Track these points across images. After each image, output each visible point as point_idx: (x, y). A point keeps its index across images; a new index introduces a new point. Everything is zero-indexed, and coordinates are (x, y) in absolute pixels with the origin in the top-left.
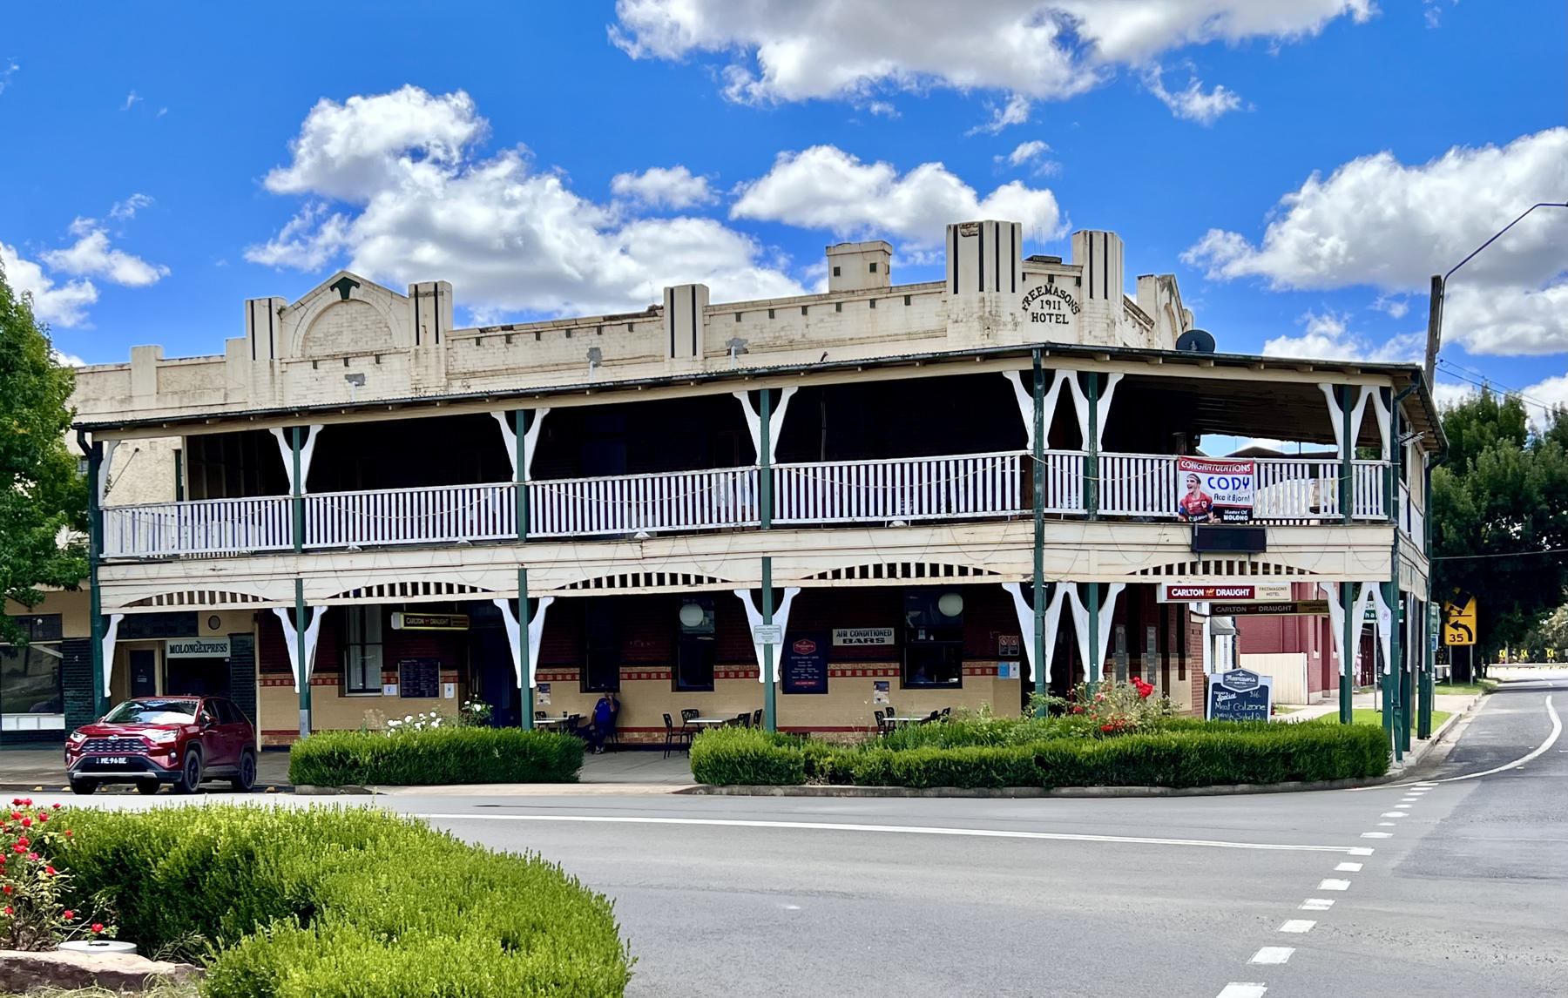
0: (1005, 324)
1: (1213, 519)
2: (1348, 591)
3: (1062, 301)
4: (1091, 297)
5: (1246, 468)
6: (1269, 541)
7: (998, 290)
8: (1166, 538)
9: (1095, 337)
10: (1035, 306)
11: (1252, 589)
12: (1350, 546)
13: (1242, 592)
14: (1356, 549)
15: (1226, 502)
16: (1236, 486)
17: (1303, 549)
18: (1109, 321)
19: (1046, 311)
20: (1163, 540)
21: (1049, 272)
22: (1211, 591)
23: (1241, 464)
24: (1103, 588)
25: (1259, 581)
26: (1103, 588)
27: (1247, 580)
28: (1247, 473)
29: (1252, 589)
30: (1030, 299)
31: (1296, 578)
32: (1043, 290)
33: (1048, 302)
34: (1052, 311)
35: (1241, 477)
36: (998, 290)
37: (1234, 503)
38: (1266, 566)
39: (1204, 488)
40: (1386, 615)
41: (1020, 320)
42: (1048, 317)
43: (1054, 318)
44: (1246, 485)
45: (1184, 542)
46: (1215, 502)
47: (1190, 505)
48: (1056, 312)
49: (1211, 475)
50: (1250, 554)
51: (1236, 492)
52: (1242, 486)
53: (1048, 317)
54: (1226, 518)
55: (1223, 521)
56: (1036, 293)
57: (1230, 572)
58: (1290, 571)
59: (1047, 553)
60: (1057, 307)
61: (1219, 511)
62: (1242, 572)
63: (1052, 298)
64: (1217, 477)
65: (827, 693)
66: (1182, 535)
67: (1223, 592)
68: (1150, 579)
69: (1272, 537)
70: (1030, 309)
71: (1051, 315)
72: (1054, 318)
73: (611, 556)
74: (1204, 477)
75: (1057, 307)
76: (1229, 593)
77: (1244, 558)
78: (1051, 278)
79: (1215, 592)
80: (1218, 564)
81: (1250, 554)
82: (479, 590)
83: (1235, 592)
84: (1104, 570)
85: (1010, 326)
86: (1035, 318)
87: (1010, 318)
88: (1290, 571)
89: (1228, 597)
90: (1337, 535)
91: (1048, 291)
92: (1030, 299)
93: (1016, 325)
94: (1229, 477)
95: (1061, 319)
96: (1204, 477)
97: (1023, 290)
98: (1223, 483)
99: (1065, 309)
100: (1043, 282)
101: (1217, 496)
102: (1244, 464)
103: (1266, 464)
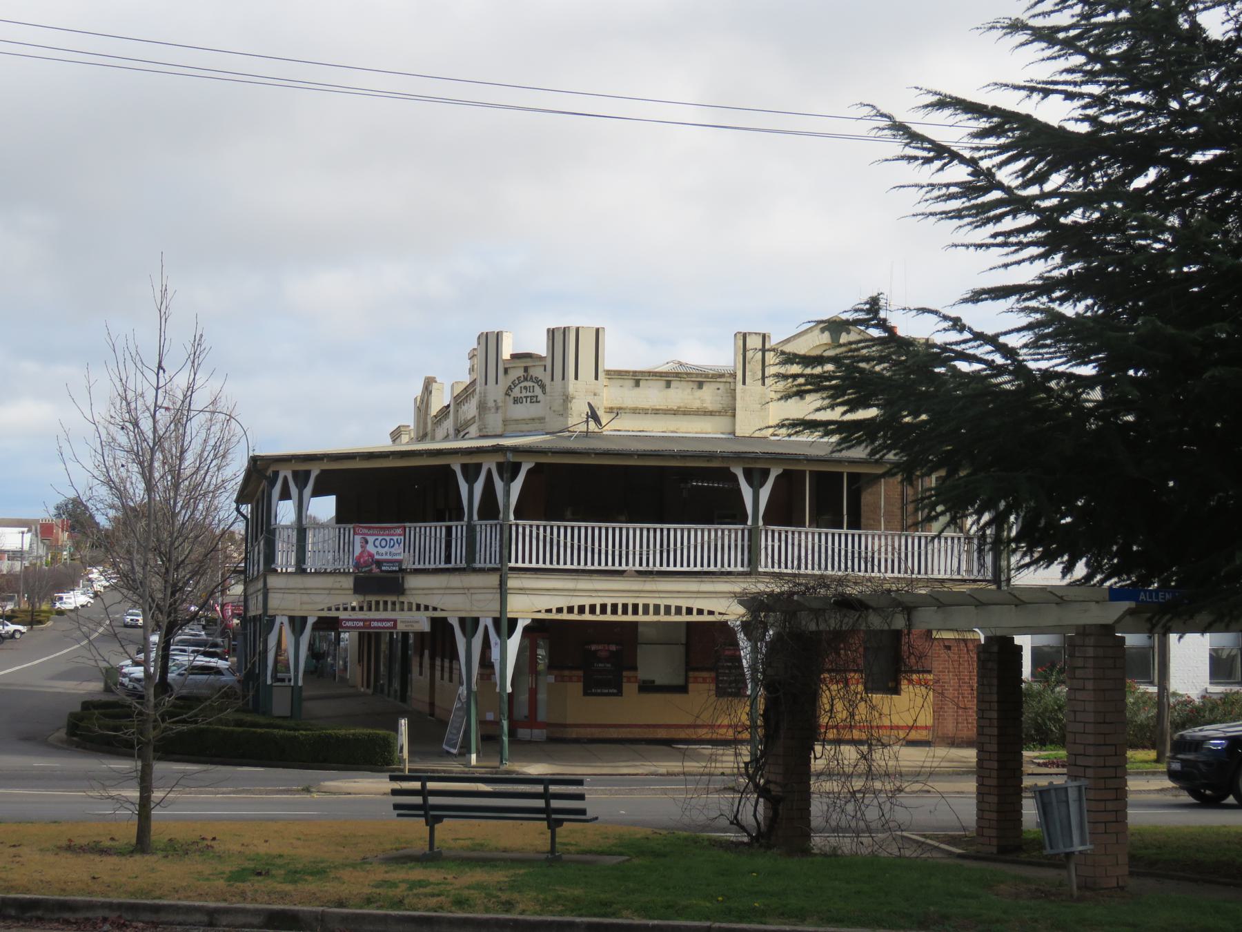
0: (490, 409)
2: (469, 625)
3: (536, 385)
4: (552, 379)
5: (399, 531)
6: (406, 586)
7: (486, 384)
9: (554, 411)
10: (516, 392)
11: (395, 621)
12: (468, 589)
13: (388, 624)
14: (472, 591)
15: (384, 557)
16: (392, 544)
17: (435, 592)
19: (524, 394)
20: (337, 585)
21: (525, 365)
22: (368, 623)
23: (392, 528)
24: (304, 619)
25: (406, 615)
26: (304, 619)
28: (400, 535)
29: (395, 621)
30: (513, 387)
31: (431, 614)
32: (522, 379)
33: (525, 388)
35: (395, 538)
36: (486, 384)
37: (390, 558)
38: (410, 604)
40: (496, 644)
41: (500, 404)
42: (524, 400)
43: (529, 399)
46: (377, 557)
47: (362, 560)
51: (393, 550)
52: (397, 545)
53: (524, 400)
54: (383, 568)
55: (382, 571)
56: (517, 382)
57: (385, 609)
58: (427, 608)
59: (271, 595)
61: (379, 563)
62: (377, 609)
63: (531, 384)
64: (380, 538)
65: (622, 696)
66: (348, 582)
67: (375, 624)
68: (333, 614)
69: (412, 582)
70: (513, 395)
71: (526, 397)
72: (529, 399)
73: (444, 585)
74: (371, 539)
76: (380, 624)
77: (394, 598)
78: (526, 369)
80: (377, 603)
84: (305, 607)
85: (493, 410)
86: (516, 401)
87: (493, 404)
88: (427, 608)
89: (380, 628)
90: (455, 581)
91: (526, 379)
92: (513, 387)
93: (497, 408)
94: (388, 538)
95: (535, 399)
96: (371, 539)
97: (504, 382)
98: (383, 543)
99: (538, 391)
100: (521, 373)
101: (378, 553)
102: (399, 528)
103: (486, 525)
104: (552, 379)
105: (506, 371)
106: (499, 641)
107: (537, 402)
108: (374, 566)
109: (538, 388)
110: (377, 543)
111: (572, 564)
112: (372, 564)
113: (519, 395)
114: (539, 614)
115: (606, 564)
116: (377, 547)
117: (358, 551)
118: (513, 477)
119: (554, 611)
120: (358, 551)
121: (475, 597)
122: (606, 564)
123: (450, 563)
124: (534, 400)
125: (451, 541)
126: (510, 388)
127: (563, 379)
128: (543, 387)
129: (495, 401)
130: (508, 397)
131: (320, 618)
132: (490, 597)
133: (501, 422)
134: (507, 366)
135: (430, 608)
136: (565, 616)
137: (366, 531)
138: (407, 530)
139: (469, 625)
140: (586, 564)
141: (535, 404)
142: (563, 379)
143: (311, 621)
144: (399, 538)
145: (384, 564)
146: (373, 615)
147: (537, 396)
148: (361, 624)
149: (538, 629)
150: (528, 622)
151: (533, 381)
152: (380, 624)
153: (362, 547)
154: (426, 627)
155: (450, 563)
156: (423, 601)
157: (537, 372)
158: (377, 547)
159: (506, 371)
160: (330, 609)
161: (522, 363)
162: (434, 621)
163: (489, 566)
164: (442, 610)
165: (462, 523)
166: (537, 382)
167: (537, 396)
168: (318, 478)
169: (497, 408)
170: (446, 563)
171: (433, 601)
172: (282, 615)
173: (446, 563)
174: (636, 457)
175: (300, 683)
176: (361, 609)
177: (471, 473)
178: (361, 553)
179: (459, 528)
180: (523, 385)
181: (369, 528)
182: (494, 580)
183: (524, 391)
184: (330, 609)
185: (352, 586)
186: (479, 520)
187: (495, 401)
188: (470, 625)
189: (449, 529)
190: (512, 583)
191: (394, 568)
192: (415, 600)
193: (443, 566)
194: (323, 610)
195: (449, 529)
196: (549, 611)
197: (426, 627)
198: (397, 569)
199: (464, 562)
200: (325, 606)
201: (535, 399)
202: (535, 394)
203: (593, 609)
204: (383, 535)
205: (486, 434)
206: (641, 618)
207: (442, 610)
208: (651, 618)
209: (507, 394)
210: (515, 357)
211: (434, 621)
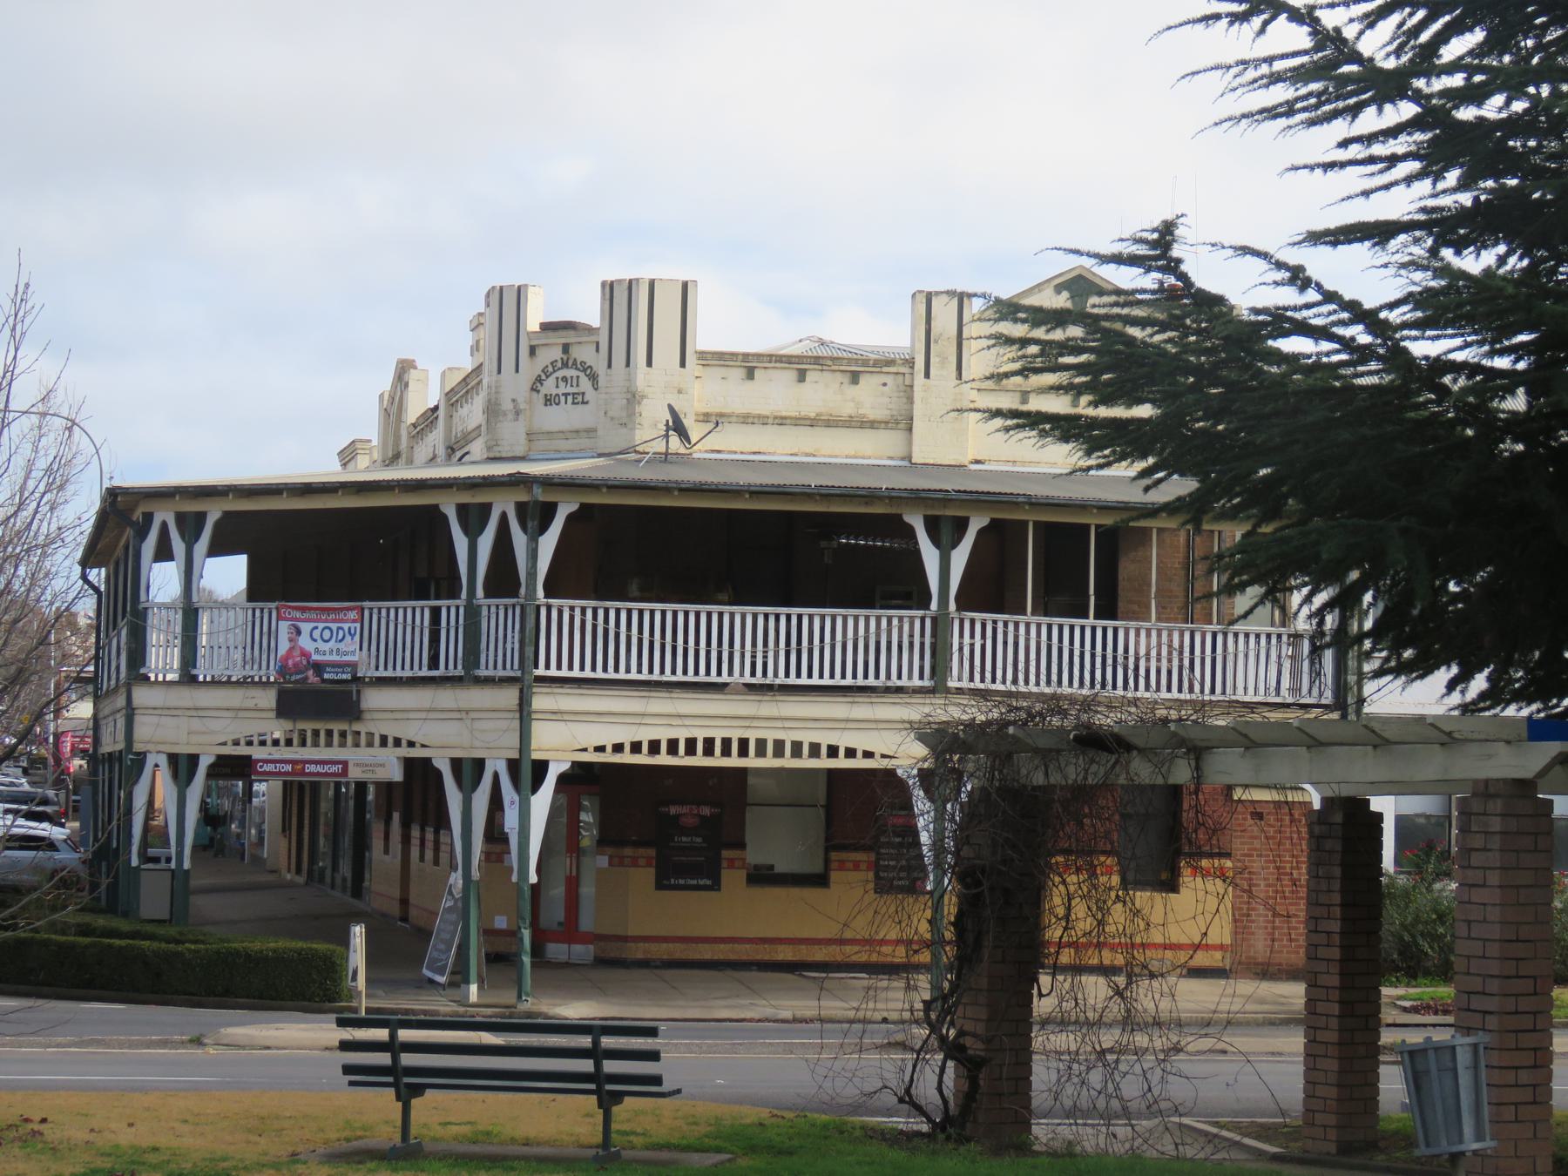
0: (505, 414)
1: (312, 677)
2: (467, 771)
3: (582, 375)
4: (610, 366)
5: (353, 615)
6: (364, 705)
7: (499, 372)
8: (254, 701)
9: (612, 419)
10: (549, 387)
11: (345, 764)
12: (467, 712)
13: (334, 769)
14: (473, 715)
16: (340, 637)
17: (411, 715)
18: (629, 396)
19: (563, 389)
20: (250, 704)
22: (299, 767)
23: (341, 609)
24: (193, 760)
26: (193, 760)
27: (335, 753)
28: (354, 621)
29: (345, 764)
30: (543, 377)
31: (405, 752)
32: (559, 365)
33: (565, 379)
34: (570, 390)
35: (346, 626)
36: (499, 372)
38: (370, 735)
39: (305, 642)
40: (512, 803)
41: (522, 407)
42: (563, 398)
43: (570, 399)
44: (353, 636)
45: (269, 707)
46: (315, 657)
47: (290, 662)
48: (574, 390)
49: (316, 624)
50: (350, 723)
51: (342, 646)
52: (348, 638)
53: (563, 398)
54: (326, 676)
55: (324, 681)
56: (550, 369)
57: (329, 744)
58: (397, 742)
59: (138, 719)
60: (575, 384)
61: (319, 668)
62: (316, 744)
64: (321, 626)
65: (719, 890)
66: (268, 699)
67: (312, 768)
68: (242, 750)
69: (374, 699)
71: (566, 395)
72: (570, 399)
73: (427, 705)
74: (306, 627)
75: (575, 384)
76: (319, 769)
77: (344, 726)
78: (566, 348)
79: (304, 768)
80: (316, 733)
81: (350, 723)
82: (417, 745)
83: (326, 767)
84: (195, 739)
85: (511, 416)
86: (548, 400)
89: (318, 774)
90: (446, 698)
91: (565, 365)
92: (543, 377)
93: (518, 413)
94: (334, 626)
95: (580, 398)
96: (306, 627)
97: (530, 369)
98: (327, 634)
99: (585, 384)
100: (556, 354)
102: (348, 609)
103: (497, 606)
104: (610, 366)
105: (533, 351)
106: (517, 798)
107: (583, 403)
108: (310, 673)
109: (586, 379)
110: (316, 634)
111: (639, 671)
112: (307, 669)
113: (554, 392)
114: (585, 753)
115: (696, 673)
116: (315, 640)
117: (284, 647)
118: (544, 527)
119: (609, 749)
120: (284, 647)
121: (477, 725)
122: (696, 673)
123: (437, 668)
124: (579, 399)
125: (438, 631)
126: (539, 380)
127: (628, 364)
128: (593, 378)
129: (513, 400)
130: (535, 394)
131: (220, 757)
132: (504, 724)
133: (524, 436)
134: (534, 343)
135: (404, 743)
136: (627, 758)
137: (298, 614)
138: (367, 613)
139: (467, 771)
140: (662, 672)
141: (580, 406)
142: (628, 364)
143: (205, 763)
144: (353, 625)
145: (328, 669)
146: (308, 753)
147: (583, 394)
148: (289, 768)
149: (581, 778)
150: (565, 767)
151: (577, 369)
152: (319, 769)
153: (291, 640)
154: (397, 775)
155: (437, 668)
156: (391, 731)
157: (583, 353)
158: (315, 640)
159: (533, 351)
160: (236, 743)
161: (560, 338)
162: (409, 764)
163: (500, 673)
164: (423, 746)
165: (457, 602)
166: (584, 370)
167: (583, 394)
168: (218, 525)
169: (518, 413)
170: (430, 668)
171: (407, 732)
172: (158, 752)
173: (430, 668)
174: (747, 496)
175: (187, 865)
176: (289, 743)
177: (474, 518)
178: (291, 649)
179: (452, 611)
180: (560, 374)
181: (303, 610)
182: (510, 696)
183: (562, 384)
184: (236, 743)
185: (274, 705)
186: (487, 596)
187: (513, 400)
188: (469, 771)
189: (436, 612)
190: (542, 701)
191: (344, 677)
192: (379, 728)
193: (425, 672)
194: (225, 744)
195: (436, 612)
196: (600, 749)
197: (397, 775)
198: (349, 677)
199: (460, 667)
200: (229, 738)
201: (580, 398)
202: (581, 389)
203: (673, 746)
204: (326, 621)
205: (498, 455)
206: (752, 762)
207: (423, 746)
208: (769, 762)
209: (534, 389)
210: (547, 327)
211: (409, 764)
